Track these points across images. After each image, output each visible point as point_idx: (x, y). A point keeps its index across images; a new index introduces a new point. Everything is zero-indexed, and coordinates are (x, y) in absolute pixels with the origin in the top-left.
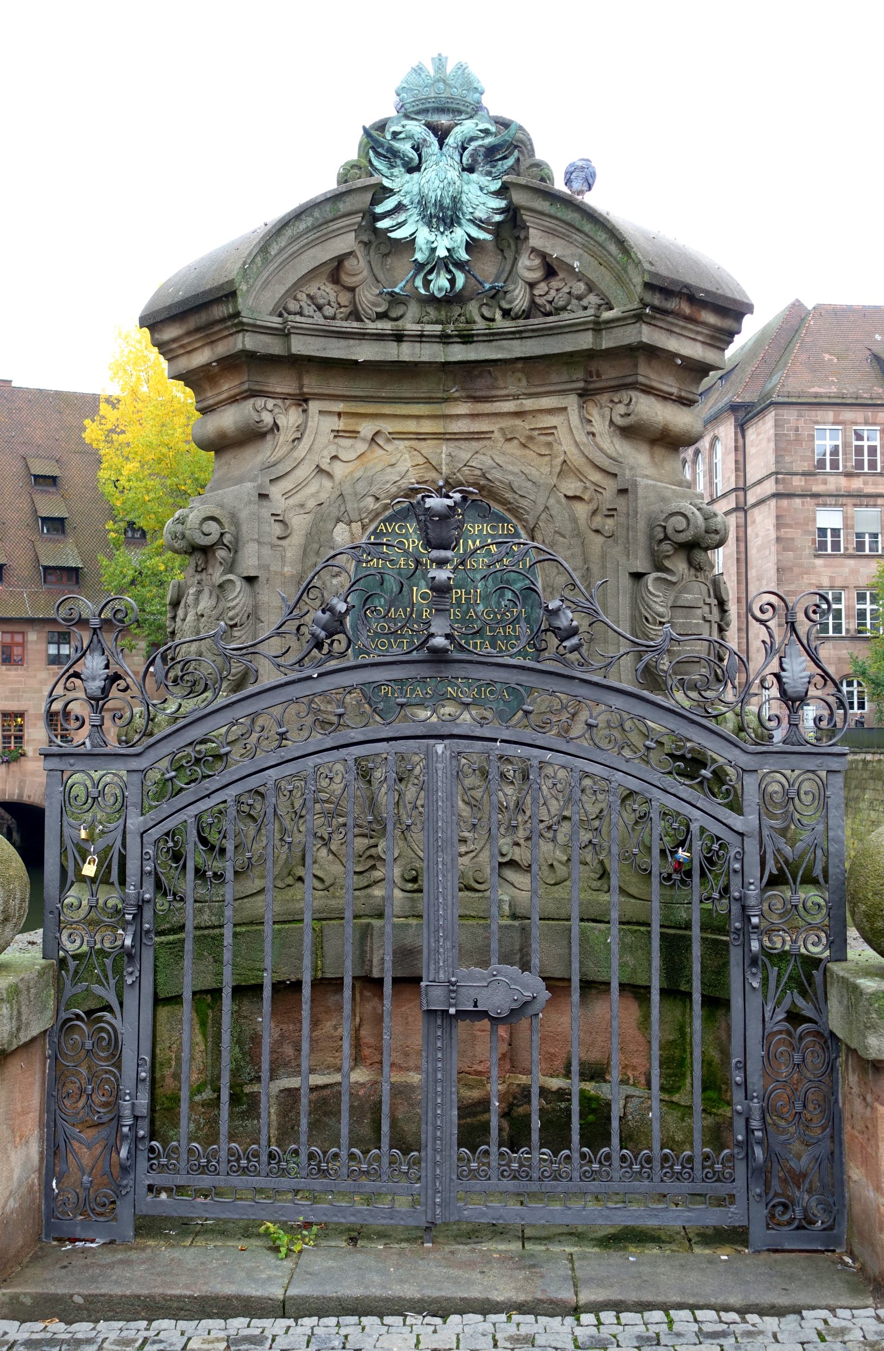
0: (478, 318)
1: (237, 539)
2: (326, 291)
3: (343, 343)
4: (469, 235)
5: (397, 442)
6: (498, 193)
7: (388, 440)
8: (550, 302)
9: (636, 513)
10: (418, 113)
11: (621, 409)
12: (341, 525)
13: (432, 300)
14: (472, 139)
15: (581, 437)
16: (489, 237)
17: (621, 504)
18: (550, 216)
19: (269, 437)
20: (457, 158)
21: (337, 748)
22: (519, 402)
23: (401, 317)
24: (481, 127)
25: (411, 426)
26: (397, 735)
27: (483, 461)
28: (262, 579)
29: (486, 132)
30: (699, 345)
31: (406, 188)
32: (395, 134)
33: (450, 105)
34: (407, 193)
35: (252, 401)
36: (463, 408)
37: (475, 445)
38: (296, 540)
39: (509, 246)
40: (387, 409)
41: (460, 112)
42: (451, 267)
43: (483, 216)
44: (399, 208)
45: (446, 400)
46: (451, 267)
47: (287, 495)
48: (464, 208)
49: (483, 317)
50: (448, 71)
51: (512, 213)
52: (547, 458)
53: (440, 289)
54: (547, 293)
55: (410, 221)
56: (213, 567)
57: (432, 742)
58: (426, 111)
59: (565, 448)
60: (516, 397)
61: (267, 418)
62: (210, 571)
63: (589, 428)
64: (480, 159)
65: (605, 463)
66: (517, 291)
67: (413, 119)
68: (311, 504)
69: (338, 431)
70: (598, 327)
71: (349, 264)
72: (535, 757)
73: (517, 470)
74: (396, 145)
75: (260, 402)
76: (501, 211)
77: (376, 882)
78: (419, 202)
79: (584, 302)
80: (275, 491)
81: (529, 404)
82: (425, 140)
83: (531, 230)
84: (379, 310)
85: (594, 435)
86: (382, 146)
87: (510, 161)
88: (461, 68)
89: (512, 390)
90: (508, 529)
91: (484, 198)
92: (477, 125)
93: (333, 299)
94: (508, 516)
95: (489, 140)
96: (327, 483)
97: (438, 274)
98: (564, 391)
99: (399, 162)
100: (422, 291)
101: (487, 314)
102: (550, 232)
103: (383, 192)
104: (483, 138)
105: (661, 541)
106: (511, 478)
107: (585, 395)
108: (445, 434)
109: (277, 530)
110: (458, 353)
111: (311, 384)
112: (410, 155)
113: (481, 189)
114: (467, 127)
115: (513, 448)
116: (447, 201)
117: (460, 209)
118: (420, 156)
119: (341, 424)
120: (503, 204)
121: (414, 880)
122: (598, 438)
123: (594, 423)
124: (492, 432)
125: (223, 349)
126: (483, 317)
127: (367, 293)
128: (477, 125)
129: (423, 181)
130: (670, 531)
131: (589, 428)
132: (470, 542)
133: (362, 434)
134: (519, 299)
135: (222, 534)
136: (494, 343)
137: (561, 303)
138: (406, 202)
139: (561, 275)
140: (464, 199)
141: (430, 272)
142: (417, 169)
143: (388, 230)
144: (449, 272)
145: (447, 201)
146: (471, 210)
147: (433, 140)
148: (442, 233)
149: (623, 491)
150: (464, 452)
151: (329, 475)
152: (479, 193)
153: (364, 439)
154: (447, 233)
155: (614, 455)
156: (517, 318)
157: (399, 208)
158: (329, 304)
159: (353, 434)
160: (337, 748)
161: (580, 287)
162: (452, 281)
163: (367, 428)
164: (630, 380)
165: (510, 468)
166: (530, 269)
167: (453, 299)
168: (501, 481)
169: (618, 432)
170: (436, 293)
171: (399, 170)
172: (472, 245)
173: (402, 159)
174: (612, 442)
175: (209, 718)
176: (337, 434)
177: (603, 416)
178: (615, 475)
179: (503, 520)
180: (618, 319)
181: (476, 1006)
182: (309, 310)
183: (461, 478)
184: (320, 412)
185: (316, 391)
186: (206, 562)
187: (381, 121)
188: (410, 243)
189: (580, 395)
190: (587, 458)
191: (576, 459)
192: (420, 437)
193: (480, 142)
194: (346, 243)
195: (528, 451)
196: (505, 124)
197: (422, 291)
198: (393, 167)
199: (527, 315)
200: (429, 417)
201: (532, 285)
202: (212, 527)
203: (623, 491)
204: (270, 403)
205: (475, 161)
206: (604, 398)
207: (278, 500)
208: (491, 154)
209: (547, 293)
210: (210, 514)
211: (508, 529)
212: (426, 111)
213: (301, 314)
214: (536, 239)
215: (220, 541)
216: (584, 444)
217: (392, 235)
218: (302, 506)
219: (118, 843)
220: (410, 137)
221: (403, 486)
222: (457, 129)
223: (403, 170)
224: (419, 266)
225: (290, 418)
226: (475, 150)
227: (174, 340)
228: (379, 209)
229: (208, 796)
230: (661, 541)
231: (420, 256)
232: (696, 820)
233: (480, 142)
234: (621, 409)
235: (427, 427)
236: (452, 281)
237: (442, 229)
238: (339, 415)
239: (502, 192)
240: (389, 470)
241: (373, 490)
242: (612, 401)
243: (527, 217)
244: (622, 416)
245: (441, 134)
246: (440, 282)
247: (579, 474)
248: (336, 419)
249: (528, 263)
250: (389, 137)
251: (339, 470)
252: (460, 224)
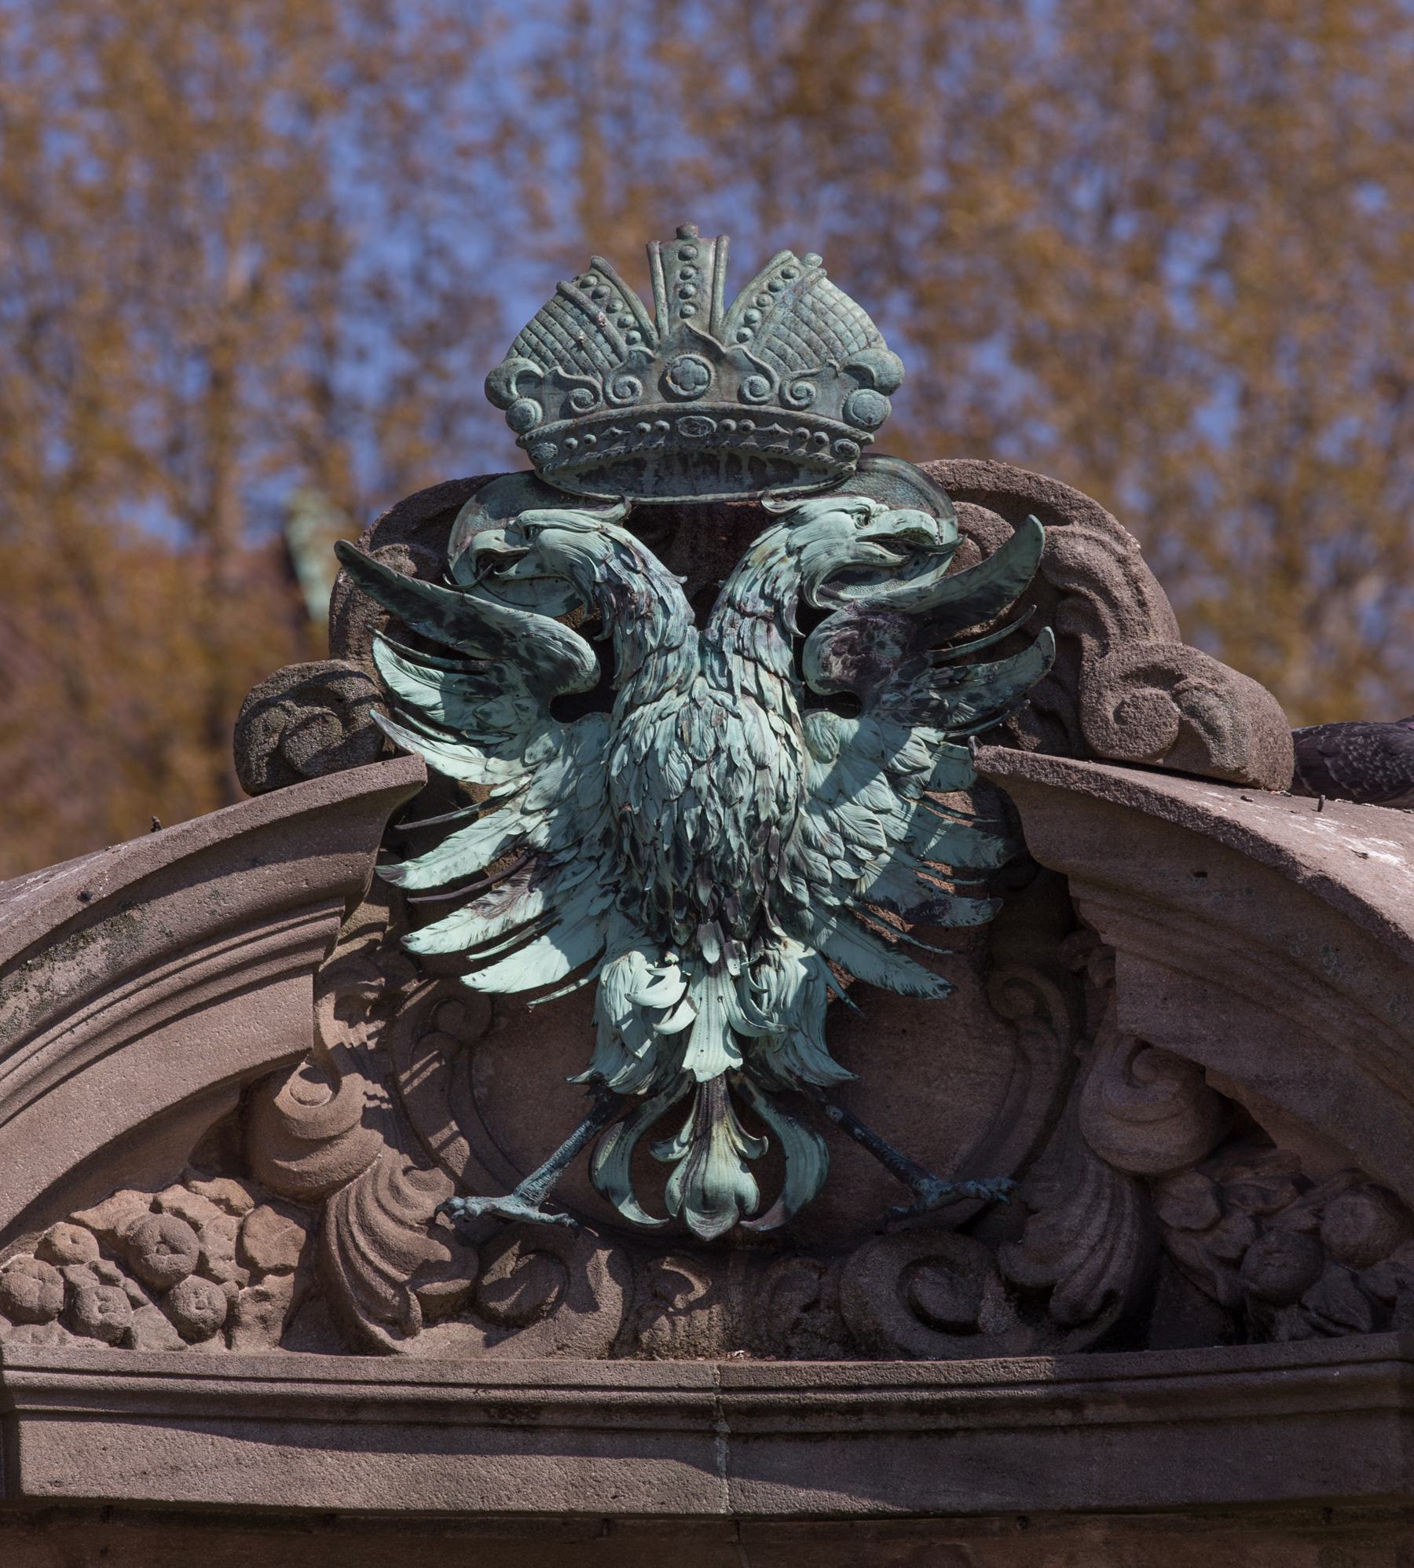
8: (1236, 1264)
20: (780, 657)
24: (887, 521)
42: (760, 1105)
46: (760, 1105)
64: (888, 654)
66: (1077, 1211)
78: (606, 838)
92: (866, 516)
93: (219, 1245)
99: (514, 674)
104: (898, 573)
118: (605, 650)
128: (866, 516)
158: (202, 1268)
173: (523, 663)
193: (883, 591)
198: (489, 691)
201: (1148, 1186)
205: (865, 668)
213: (72, 1317)
217: (486, 981)
233: (883, 591)
237: (712, 956)
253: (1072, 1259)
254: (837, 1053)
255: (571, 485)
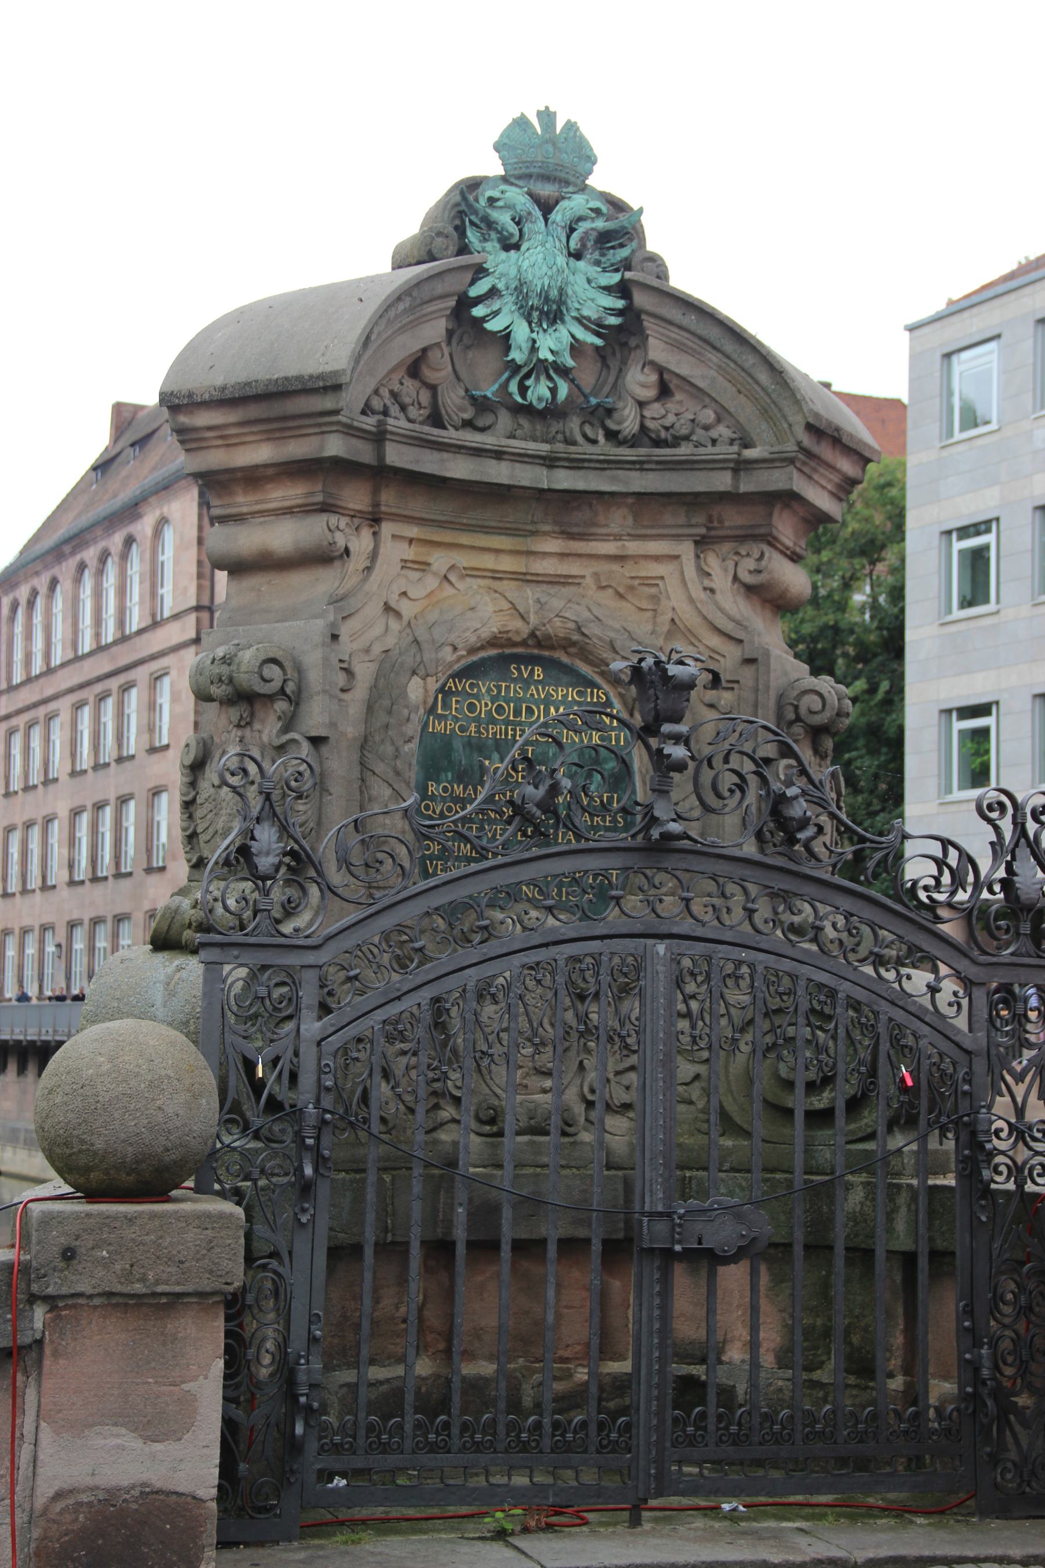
0: (580, 439)
1: (299, 691)
2: (410, 389)
3: (436, 456)
4: (573, 336)
5: (468, 580)
6: (607, 289)
7: (463, 577)
9: (768, 688)
10: (520, 177)
11: (750, 564)
12: (416, 680)
13: (527, 410)
14: (580, 219)
15: (698, 593)
16: (599, 342)
17: (747, 675)
18: (681, 327)
19: (337, 564)
20: (564, 240)
21: (546, 945)
22: (620, 543)
23: (489, 427)
25: (488, 562)
26: (612, 932)
27: (577, 613)
28: (332, 741)
29: (597, 211)
30: (826, 494)
31: (501, 268)
32: (492, 200)
33: (558, 174)
34: (502, 275)
35: (324, 517)
36: (553, 545)
37: (566, 591)
38: (360, 693)
39: (614, 354)
40: (465, 539)
41: (567, 183)
42: (551, 372)
43: (594, 316)
44: (493, 292)
45: (534, 533)
46: (551, 372)
47: (354, 637)
48: (569, 302)
49: (585, 436)
50: (558, 131)
51: (631, 316)
52: (649, 614)
53: (540, 399)
54: (663, 417)
55: (505, 310)
56: (263, 722)
57: (650, 942)
58: (529, 176)
59: (674, 603)
60: (618, 538)
61: (340, 540)
62: (257, 726)
63: (707, 583)
64: (590, 244)
65: (729, 627)
67: (512, 184)
68: (377, 649)
69: (406, 561)
70: (740, 466)
71: (434, 356)
72: (761, 962)
73: (618, 626)
74: (494, 215)
75: (333, 519)
76: (620, 313)
77: (442, 1125)
78: (516, 288)
79: (714, 434)
80: (344, 631)
81: (633, 547)
82: (529, 213)
83: (651, 340)
84: (466, 416)
85: (712, 591)
86: (476, 213)
87: (624, 253)
88: (571, 127)
89: (614, 529)
90: (598, 697)
91: (592, 293)
94: (598, 680)
95: (600, 224)
96: (394, 625)
97: (537, 379)
98: (679, 536)
100: (519, 400)
101: (590, 433)
102: (678, 346)
103: (480, 271)
104: (593, 220)
105: (791, 723)
106: (612, 635)
107: (702, 543)
108: (525, 574)
109: (341, 679)
110: (565, 480)
111: (389, 499)
112: (511, 230)
113: (589, 281)
114: (575, 204)
115: (606, 598)
116: (554, 293)
117: (565, 303)
118: (521, 231)
119: (410, 553)
120: (620, 304)
121: (492, 1121)
122: (718, 596)
123: (714, 577)
124: (583, 577)
125: (298, 449)
126: (585, 436)
127: (452, 394)
129: (526, 264)
130: (803, 711)
131: (707, 583)
132: (552, 710)
133: (434, 568)
134: (629, 422)
135: (285, 681)
136: (608, 472)
137: (684, 431)
138: (500, 286)
139: (678, 396)
140: (570, 292)
141: (528, 376)
142: (517, 247)
143: (483, 319)
144: (550, 378)
145: (554, 293)
146: (577, 306)
147: (538, 213)
148: (545, 331)
149: (750, 661)
150: (557, 600)
151: (398, 614)
152: (587, 286)
153: (435, 574)
154: (550, 331)
155: (738, 617)
156: (621, 443)
157: (493, 292)
159: (423, 566)
160: (546, 945)
161: (708, 415)
162: (554, 391)
163: (440, 561)
164: (762, 531)
165: (610, 623)
166: (644, 386)
167: (552, 412)
168: (600, 639)
169: (742, 590)
170: (535, 403)
171: (493, 245)
172: (576, 348)
174: (735, 602)
175: (400, 907)
176: (405, 564)
177: (726, 570)
178: (741, 641)
179: (593, 685)
180: (764, 461)
181: (700, 1243)
182: (394, 410)
183: (550, 631)
184: (394, 536)
185: (393, 510)
186: (252, 714)
187: (474, 178)
188: (505, 339)
189: (696, 543)
190: (705, 618)
191: (688, 616)
192: (496, 576)
194: (435, 330)
195: (624, 604)
196: (617, 206)
197: (519, 400)
199: (633, 442)
200: (512, 552)
202: (273, 672)
203: (750, 661)
204: (343, 522)
205: (584, 245)
206: (727, 547)
207: (347, 645)
208: (605, 239)
209: (663, 417)
210: (271, 655)
211: (598, 697)
212: (529, 176)
214: (657, 350)
215: (282, 691)
216: (701, 601)
218: (367, 651)
219: (290, 1053)
220: (508, 207)
221: (483, 636)
222: (564, 204)
223: (498, 246)
224: (514, 368)
225: (361, 543)
226: (586, 233)
227: (210, 428)
228: (474, 292)
229: (399, 998)
230: (791, 723)
231: (517, 355)
232: (925, 1036)
234: (750, 564)
235: (507, 564)
236: (554, 391)
237: (545, 326)
238: (411, 541)
239: (623, 290)
240: (470, 614)
241: (452, 638)
242: (737, 553)
243: (648, 323)
244: (750, 572)
245: (547, 208)
246: (539, 391)
247: (690, 637)
248: (406, 545)
249: (641, 378)
250: (483, 202)
251: (407, 609)
252: (563, 322)
253: (626, 424)
254: (573, 357)
255: (513, 180)
